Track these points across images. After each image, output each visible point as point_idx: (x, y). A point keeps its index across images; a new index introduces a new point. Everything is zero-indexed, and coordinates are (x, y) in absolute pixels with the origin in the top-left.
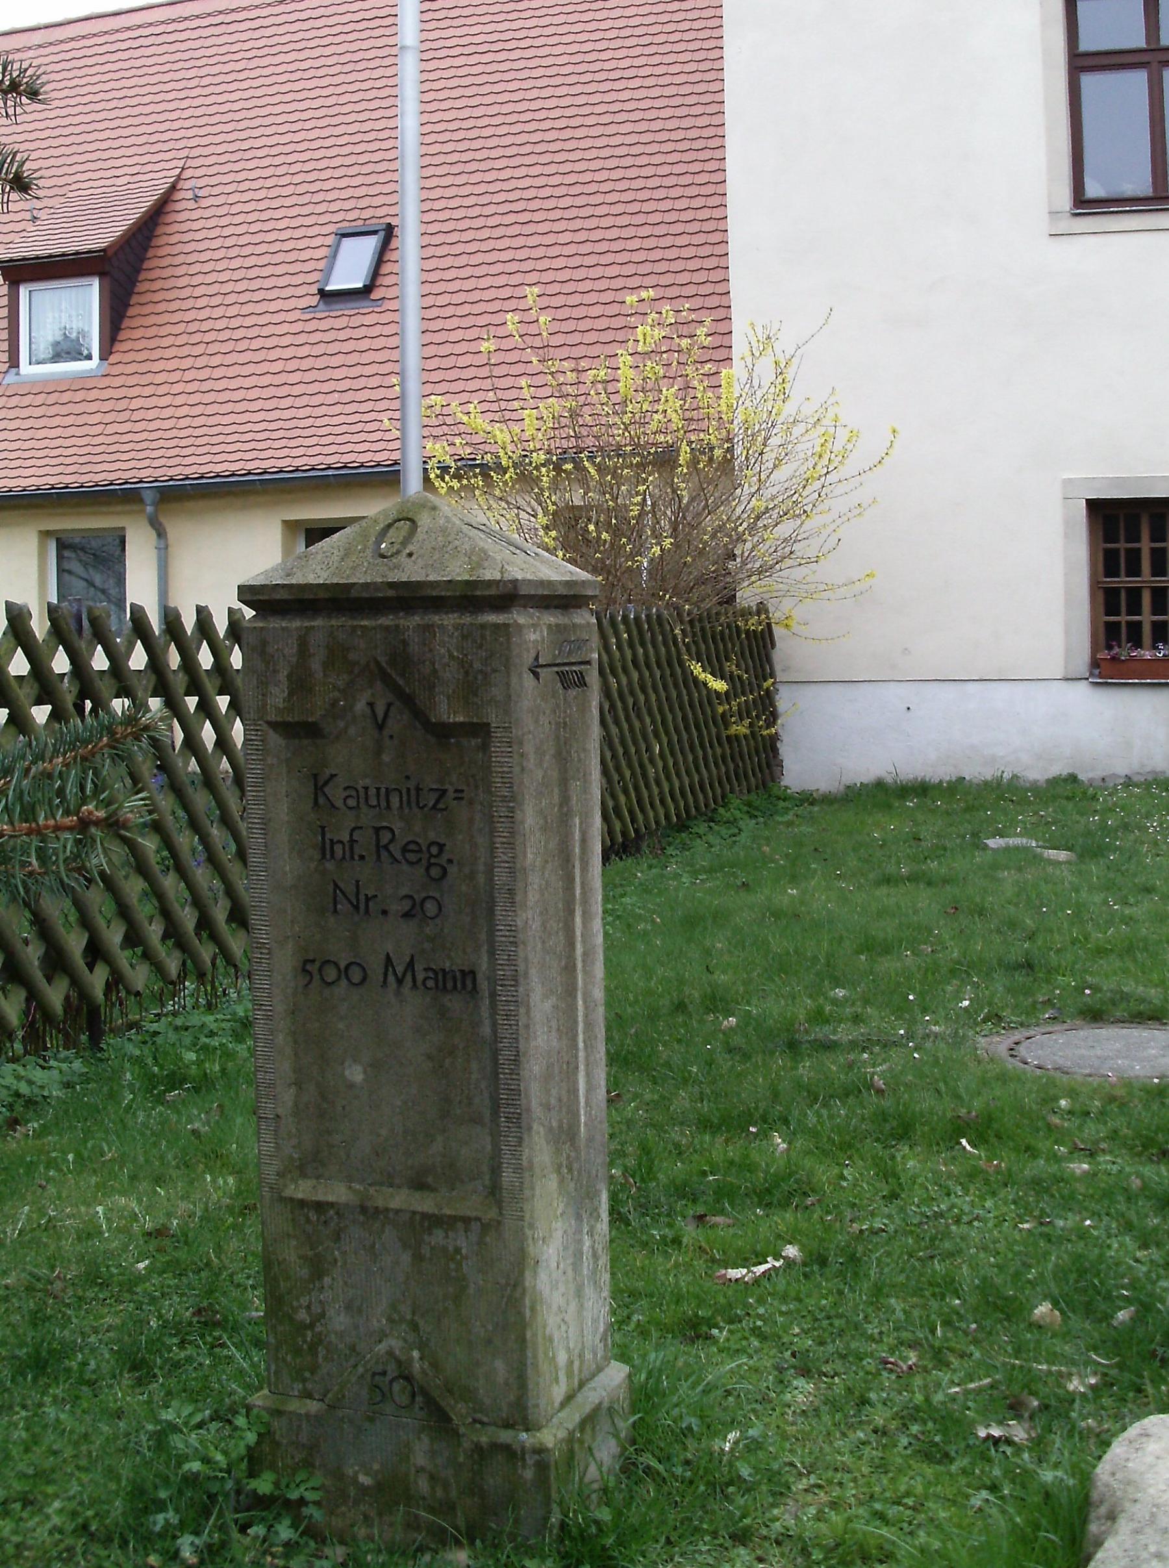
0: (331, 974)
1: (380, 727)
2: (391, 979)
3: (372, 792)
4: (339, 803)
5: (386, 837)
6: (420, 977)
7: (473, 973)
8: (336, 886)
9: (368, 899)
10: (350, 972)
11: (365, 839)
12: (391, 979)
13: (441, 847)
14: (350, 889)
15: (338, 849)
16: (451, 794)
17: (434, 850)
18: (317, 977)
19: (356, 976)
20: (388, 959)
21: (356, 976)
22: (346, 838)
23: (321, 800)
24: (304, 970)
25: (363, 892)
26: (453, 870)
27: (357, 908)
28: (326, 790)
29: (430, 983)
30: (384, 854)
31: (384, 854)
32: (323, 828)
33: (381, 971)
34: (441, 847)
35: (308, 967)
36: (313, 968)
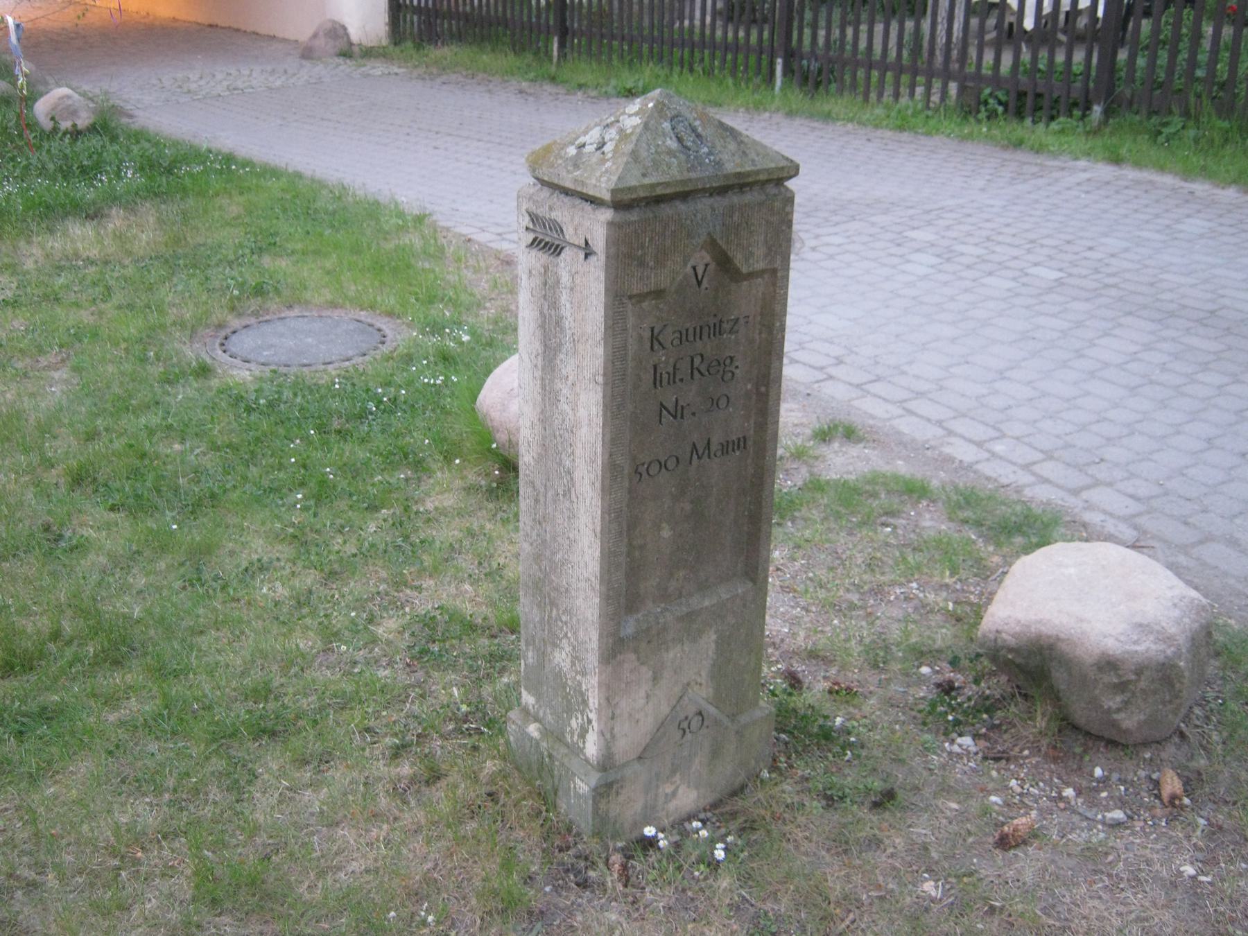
0: (654, 469)
1: (699, 283)
2: (695, 456)
3: (691, 331)
4: (668, 345)
5: (697, 361)
6: (714, 448)
7: (744, 438)
8: (662, 404)
9: (682, 407)
10: (669, 464)
11: (684, 367)
12: (695, 456)
13: (732, 358)
14: (671, 406)
15: (665, 376)
16: (742, 321)
17: (728, 361)
18: (644, 474)
19: (671, 464)
20: (694, 444)
21: (671, 464)
22: (671, 370)
23: (656, 346)
24: (636, 472)
25: (681, 403)
26: (737, 371)
27: (675, 417)
28: (660, 338)
29: (719, 453)
30: (696, 372)
31: (696, 372)
32: (655, 367)
33: (689, 455)
34: (732, 358)
35: (640, 470)
36: (643, 469)
